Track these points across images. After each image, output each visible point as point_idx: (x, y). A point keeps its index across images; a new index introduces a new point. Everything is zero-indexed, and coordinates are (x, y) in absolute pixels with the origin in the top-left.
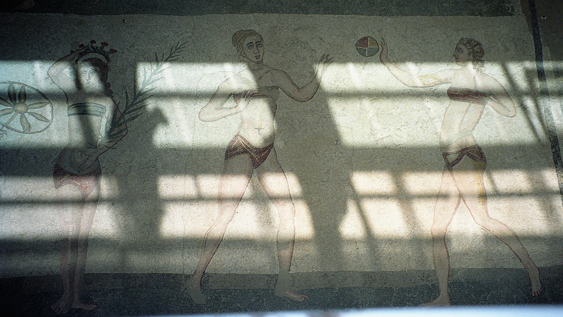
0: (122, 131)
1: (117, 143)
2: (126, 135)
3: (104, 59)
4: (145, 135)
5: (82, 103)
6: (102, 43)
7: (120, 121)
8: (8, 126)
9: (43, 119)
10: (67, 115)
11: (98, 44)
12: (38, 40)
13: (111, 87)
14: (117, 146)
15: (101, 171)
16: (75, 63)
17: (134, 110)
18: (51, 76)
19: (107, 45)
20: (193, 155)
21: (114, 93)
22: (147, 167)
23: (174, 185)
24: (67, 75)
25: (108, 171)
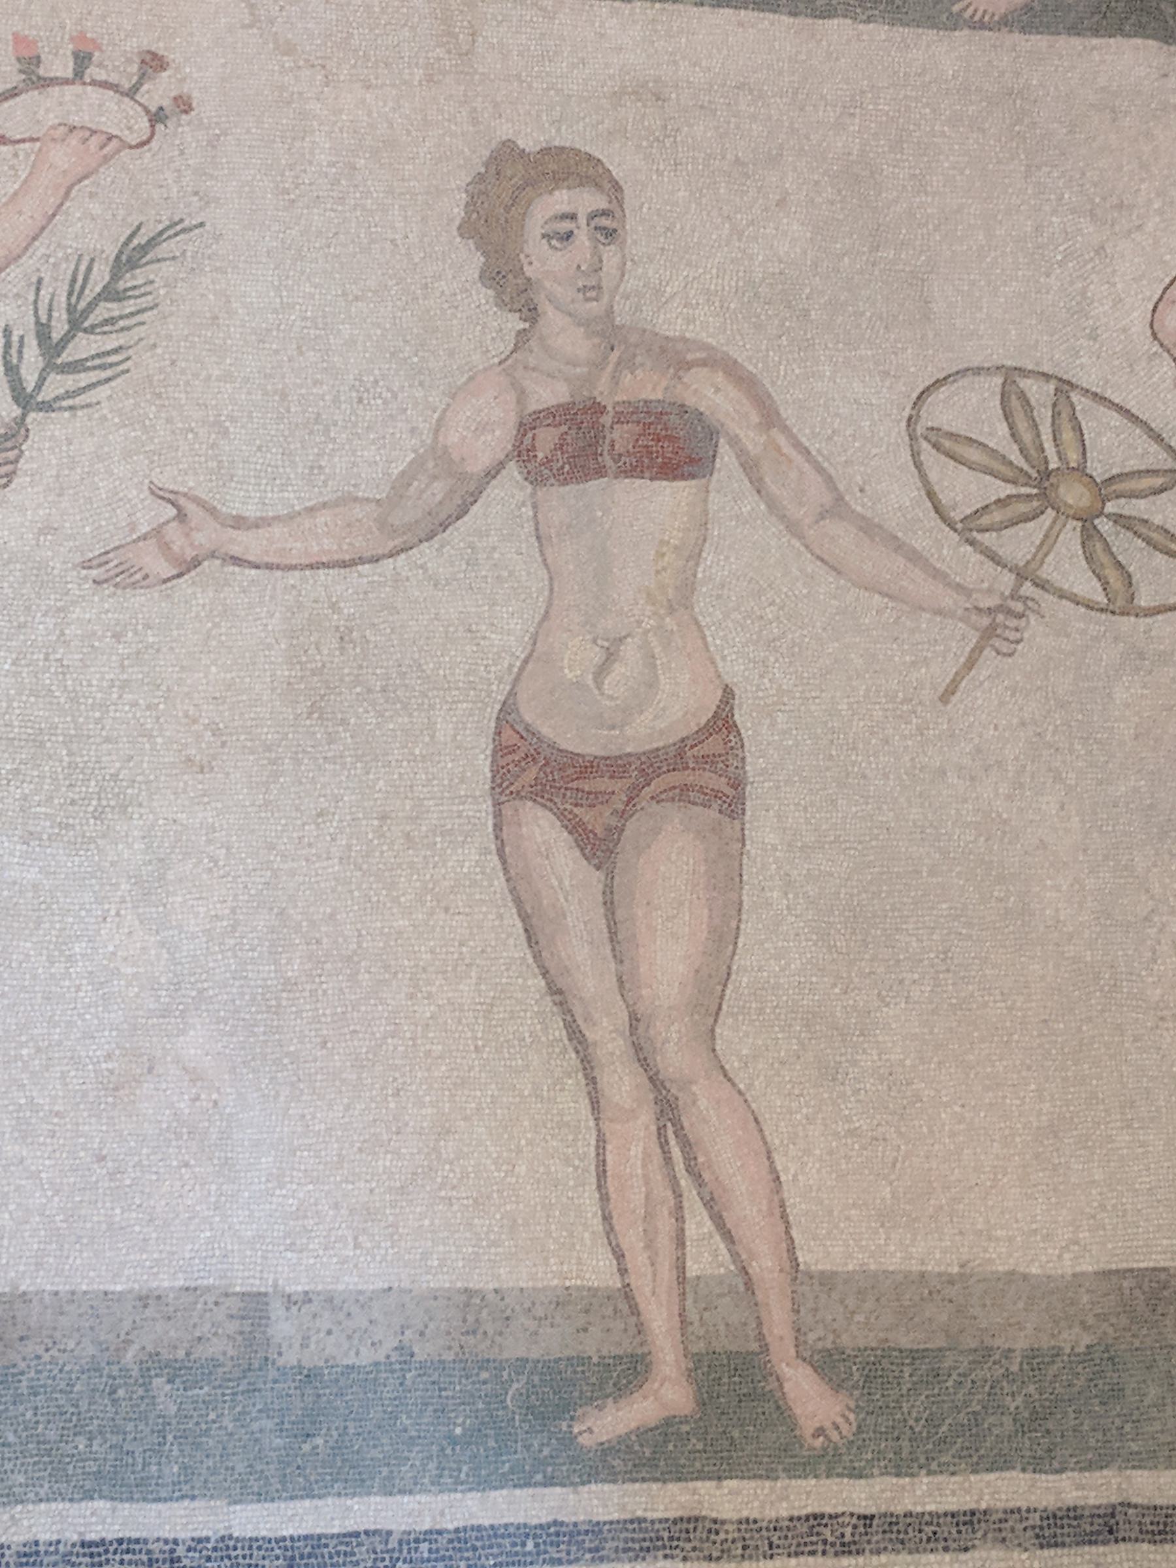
8: (1037, 577)
18: (1170, 346)
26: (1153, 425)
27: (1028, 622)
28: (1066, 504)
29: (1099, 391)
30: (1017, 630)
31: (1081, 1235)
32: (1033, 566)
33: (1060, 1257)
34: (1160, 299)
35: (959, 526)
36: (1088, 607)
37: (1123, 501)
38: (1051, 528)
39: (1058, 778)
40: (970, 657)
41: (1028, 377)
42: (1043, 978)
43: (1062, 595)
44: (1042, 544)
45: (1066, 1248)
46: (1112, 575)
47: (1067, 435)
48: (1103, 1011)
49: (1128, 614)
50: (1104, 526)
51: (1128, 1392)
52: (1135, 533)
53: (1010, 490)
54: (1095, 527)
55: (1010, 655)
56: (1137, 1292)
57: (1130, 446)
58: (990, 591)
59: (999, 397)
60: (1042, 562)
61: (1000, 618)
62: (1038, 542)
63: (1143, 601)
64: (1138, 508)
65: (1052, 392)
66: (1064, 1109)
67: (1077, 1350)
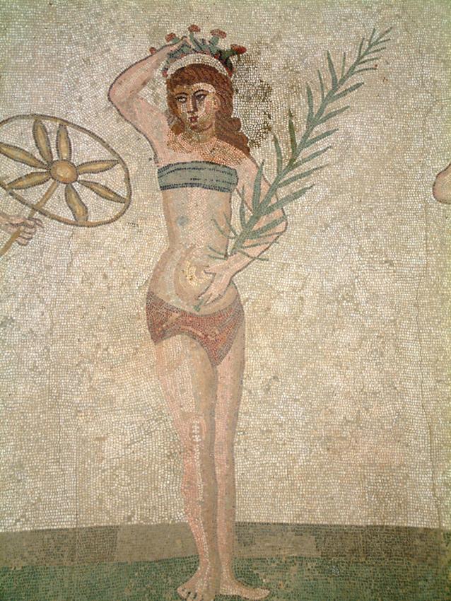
0: (275, 223)
1: (268, 248)
2: (285, 231)
3: (219, 67)
4: (324, 231)
5: (185, 163)
6: (212, 32)
7: (269, 201)
9: (112, 196)
10: (159, 187)
11: (205, 34)
12: (81, 25)
13: (242, 129)
14: (269, 255)
15: (242, 308)
16: (161, 76)
17: (294, 179)
18: (116, 104)
19: (223, 34)
20: (430, 274)
21: (250, 141)
22: (337, 300)
23: (397, 338)
24: (149, 101)
25: (256, 308)
26: (105, 140)
27: (36, 231)
28: (59, 176)
29: (80, 125)
30: (30, 234)
31: (27, 514)
32: (41, 204)
33: (15, 524)
34: (114, 83)
35: (7, 187)
36: (66, 223)
37: (87, 175)
38: (51, 187)
39: (42, 302)
40: (6, 246)
41: (48, 119)
42: (24, 392)
43: (53, 217)
44: (46, 194)
45: (19, 520)
46: (79, 209)
47: (63, 145)
48: (51, 408)
49: (84, 226)
50: (77, 186)
51: (40, 590)
52: (91, 189)
53: (33, 170)
54: (72, 187)
55: (25, 245)
56: (51, 541)
57: (93, 150)
58: (18, 216)
59: (31, 129)
60: (45, 203)
61: (23, 228)
62: (44, 193)
63: (91, 220)
64: (94, 178)
65: (58, 126)
66: (27, 454)
67: (17, 569)
